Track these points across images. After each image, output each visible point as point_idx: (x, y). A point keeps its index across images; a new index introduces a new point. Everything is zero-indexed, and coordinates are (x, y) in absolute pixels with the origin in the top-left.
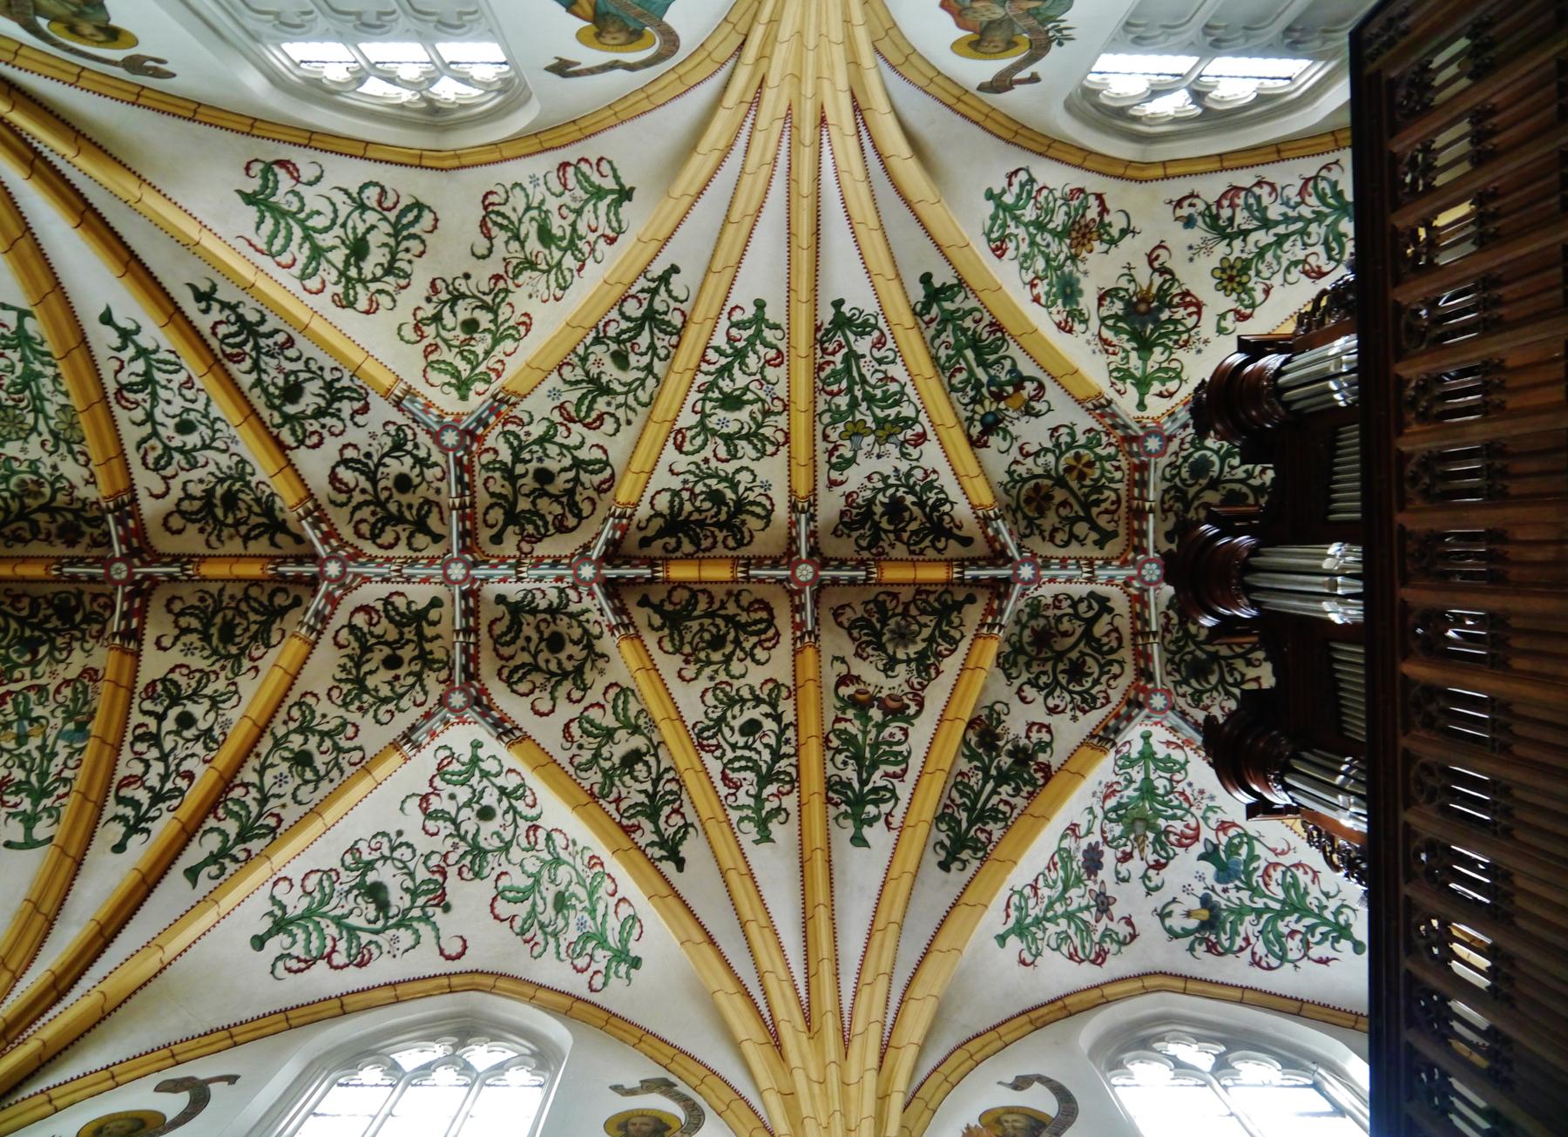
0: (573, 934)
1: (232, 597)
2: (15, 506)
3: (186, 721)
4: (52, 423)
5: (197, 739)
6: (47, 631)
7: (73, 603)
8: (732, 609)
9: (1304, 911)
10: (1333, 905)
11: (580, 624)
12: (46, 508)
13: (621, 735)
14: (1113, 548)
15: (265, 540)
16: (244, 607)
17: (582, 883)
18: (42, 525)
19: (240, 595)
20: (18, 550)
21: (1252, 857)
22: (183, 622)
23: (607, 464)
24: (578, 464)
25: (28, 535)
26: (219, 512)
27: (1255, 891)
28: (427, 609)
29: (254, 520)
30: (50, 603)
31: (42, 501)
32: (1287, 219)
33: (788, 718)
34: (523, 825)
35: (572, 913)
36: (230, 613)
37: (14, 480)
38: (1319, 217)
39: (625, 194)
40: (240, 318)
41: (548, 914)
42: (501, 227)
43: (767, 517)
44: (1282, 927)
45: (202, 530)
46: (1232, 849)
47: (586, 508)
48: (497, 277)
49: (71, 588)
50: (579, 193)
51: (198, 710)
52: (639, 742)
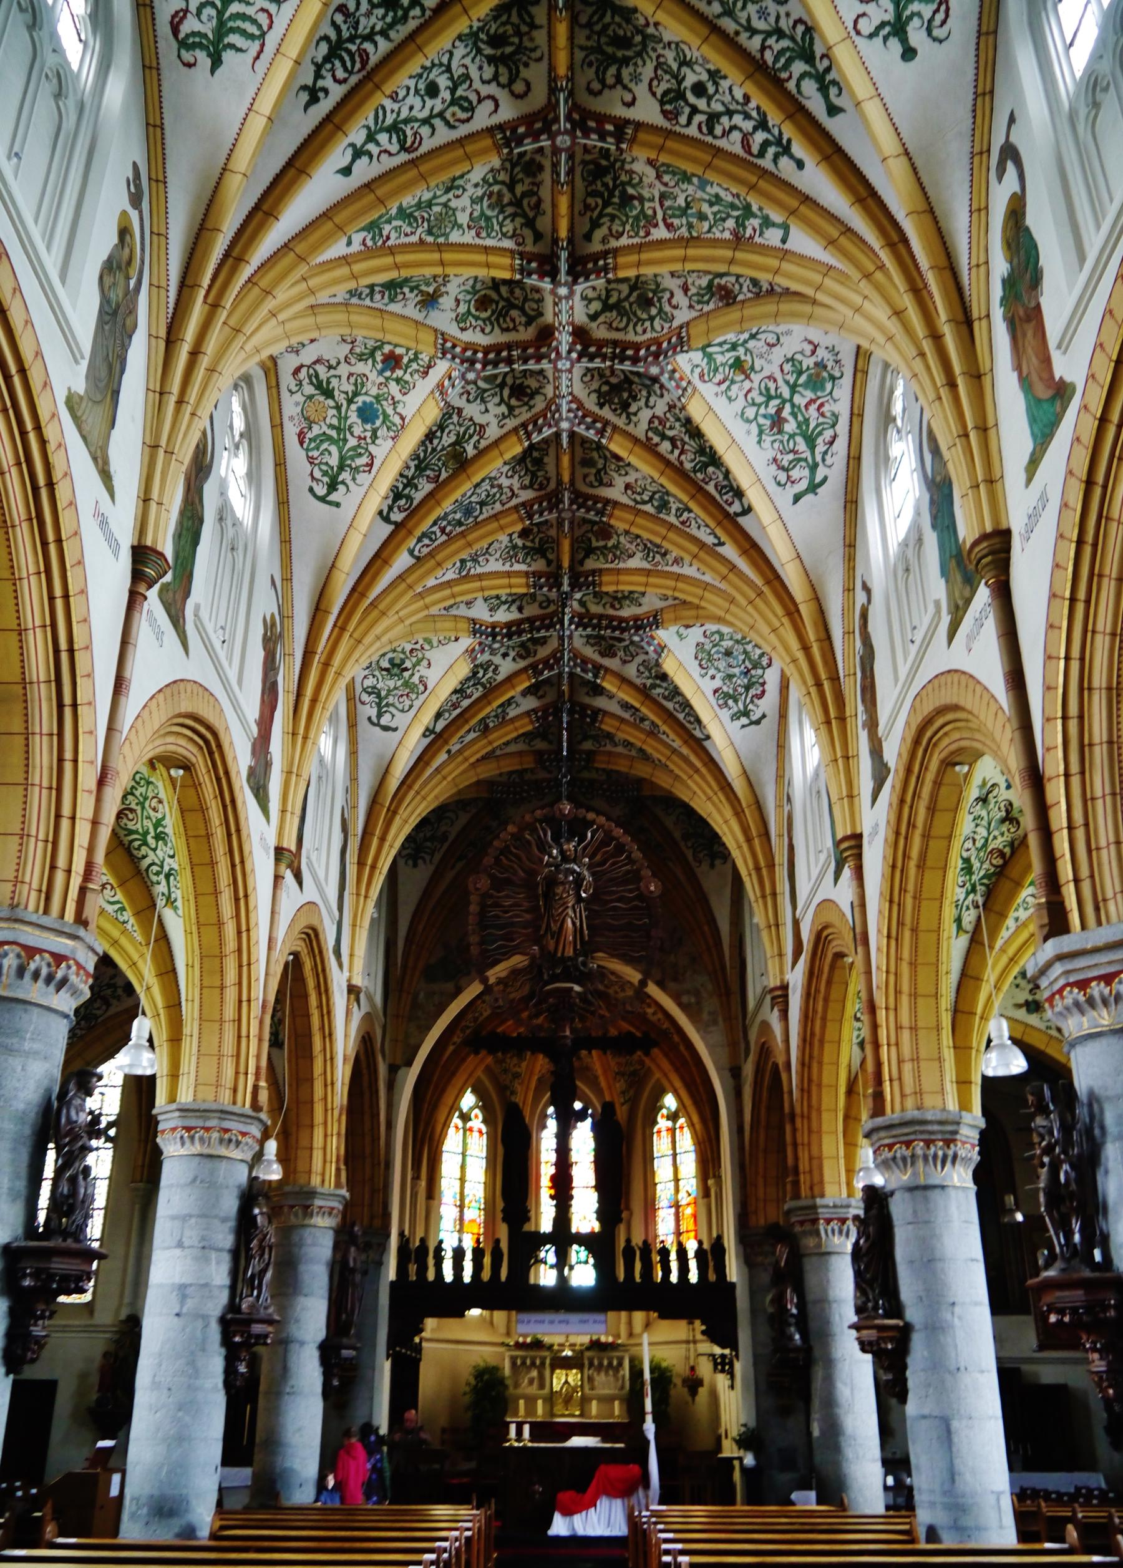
1: (588, 38)
2: (510, 210)
3: (699, 89)
4: (439, 193)
5: (716, 84)
6: (615, 187)
7: (592, 167)
12: (511, 187)
16: (598, 28)
18: (526, 188)
19: (587, 32)
20: (546, 206)
22: (610, 80)
25: (534, 199)
26: (509, 50)
29: (515, 19)
30: (593, 182)
31: (505, 190)
36: (603, 40)
37: (489, 213)
40: (327, 59)
45: (526, 65)
49: (578, 170)
51: (690, 79)
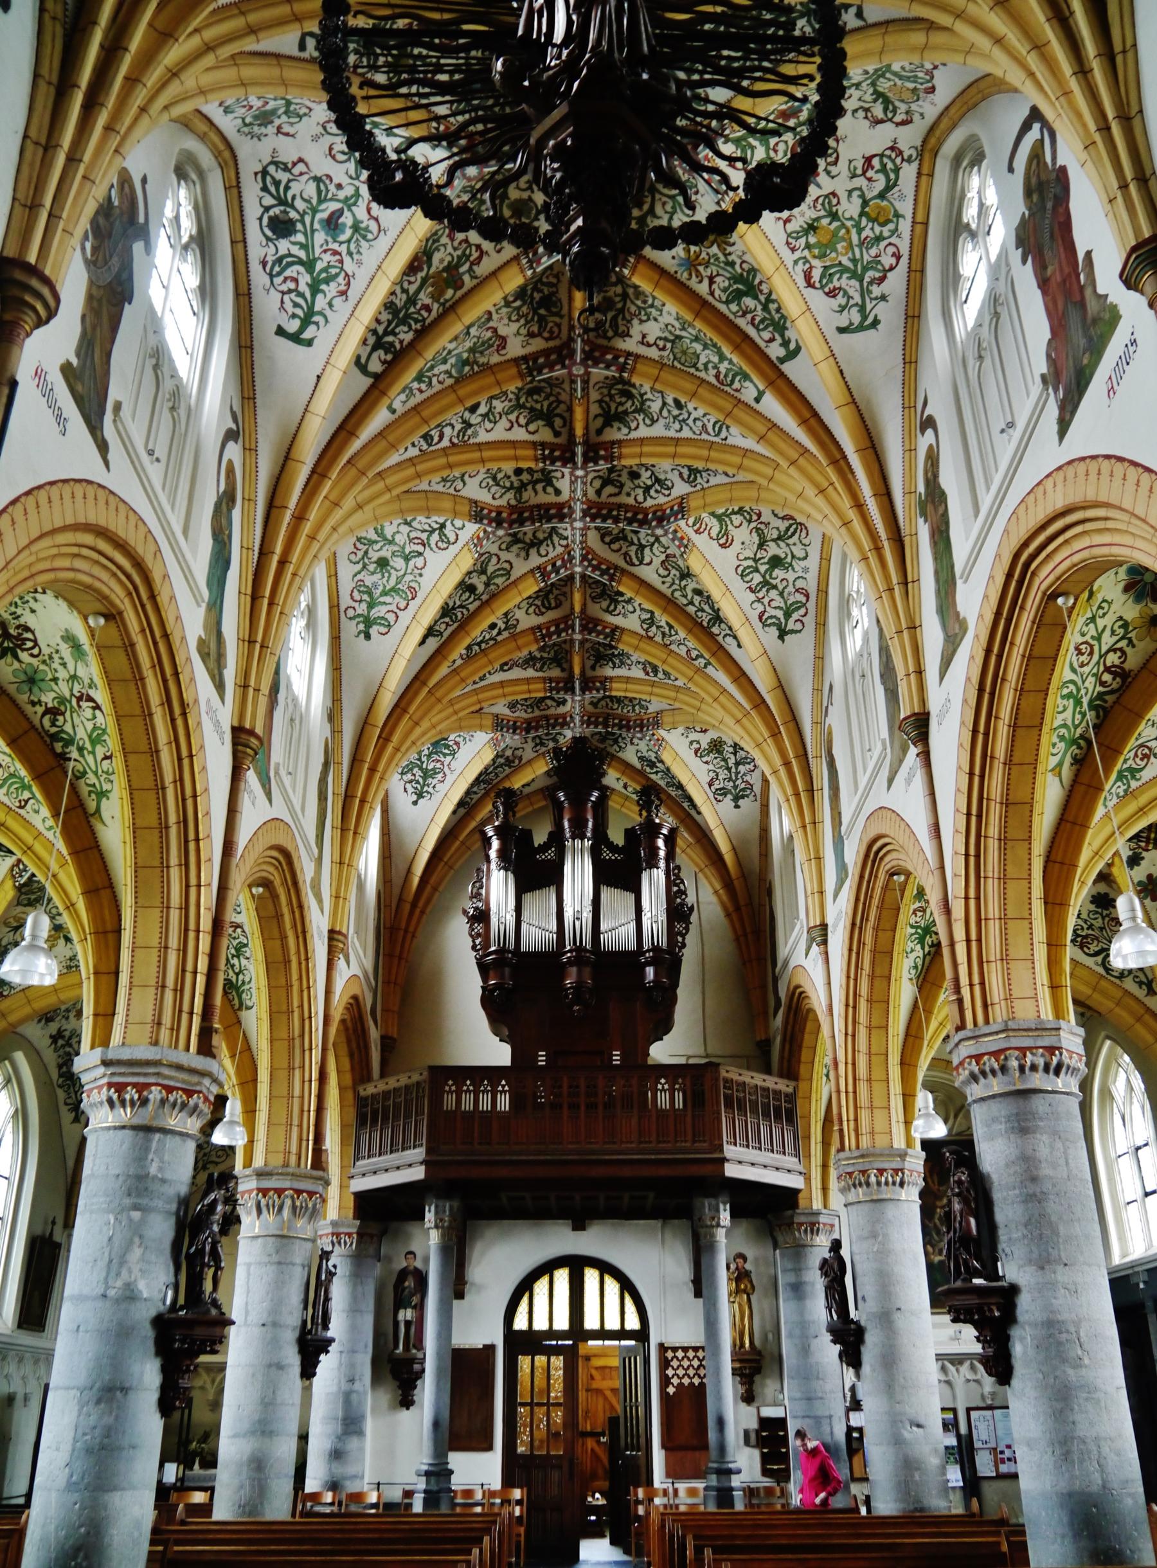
0: (369, 580)
5: (464, 422)
8: (556, 592)
9: (425, 778)
10: (430, 790)
11: (546, 539)
13: (484, 578)
14: (590, 708)
15: (599, 411)
16: (552, 399)
17: (399, 580)
21: (445, 755)
23: (641, 563)
24: (642, 547)
27: (429, 756)
28: (553, 486)
29: (613, 406)
32: (737, 773)
33: (499, 638)
34: (424, 536)
35: (379, 576)
38: (735, 787)
39: (783, 634)
41: (374, 556)
42: (788, 529)
43: (607, 611)
44: (416, 770)
46: (447, 747)
47: (615, 546)
48: (759, 515)
49: (565, 311)
50: (791, 600)
52: (481, 588)
